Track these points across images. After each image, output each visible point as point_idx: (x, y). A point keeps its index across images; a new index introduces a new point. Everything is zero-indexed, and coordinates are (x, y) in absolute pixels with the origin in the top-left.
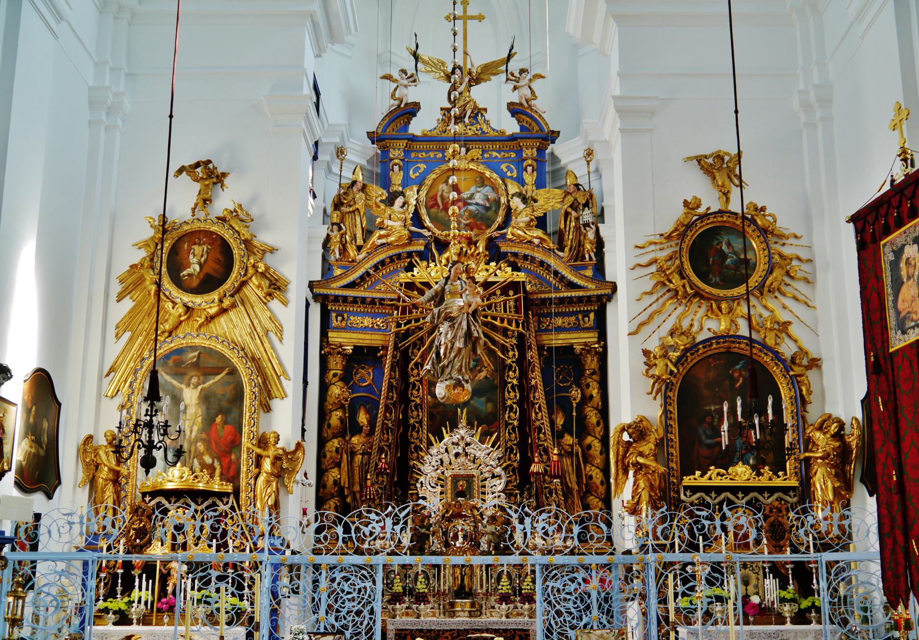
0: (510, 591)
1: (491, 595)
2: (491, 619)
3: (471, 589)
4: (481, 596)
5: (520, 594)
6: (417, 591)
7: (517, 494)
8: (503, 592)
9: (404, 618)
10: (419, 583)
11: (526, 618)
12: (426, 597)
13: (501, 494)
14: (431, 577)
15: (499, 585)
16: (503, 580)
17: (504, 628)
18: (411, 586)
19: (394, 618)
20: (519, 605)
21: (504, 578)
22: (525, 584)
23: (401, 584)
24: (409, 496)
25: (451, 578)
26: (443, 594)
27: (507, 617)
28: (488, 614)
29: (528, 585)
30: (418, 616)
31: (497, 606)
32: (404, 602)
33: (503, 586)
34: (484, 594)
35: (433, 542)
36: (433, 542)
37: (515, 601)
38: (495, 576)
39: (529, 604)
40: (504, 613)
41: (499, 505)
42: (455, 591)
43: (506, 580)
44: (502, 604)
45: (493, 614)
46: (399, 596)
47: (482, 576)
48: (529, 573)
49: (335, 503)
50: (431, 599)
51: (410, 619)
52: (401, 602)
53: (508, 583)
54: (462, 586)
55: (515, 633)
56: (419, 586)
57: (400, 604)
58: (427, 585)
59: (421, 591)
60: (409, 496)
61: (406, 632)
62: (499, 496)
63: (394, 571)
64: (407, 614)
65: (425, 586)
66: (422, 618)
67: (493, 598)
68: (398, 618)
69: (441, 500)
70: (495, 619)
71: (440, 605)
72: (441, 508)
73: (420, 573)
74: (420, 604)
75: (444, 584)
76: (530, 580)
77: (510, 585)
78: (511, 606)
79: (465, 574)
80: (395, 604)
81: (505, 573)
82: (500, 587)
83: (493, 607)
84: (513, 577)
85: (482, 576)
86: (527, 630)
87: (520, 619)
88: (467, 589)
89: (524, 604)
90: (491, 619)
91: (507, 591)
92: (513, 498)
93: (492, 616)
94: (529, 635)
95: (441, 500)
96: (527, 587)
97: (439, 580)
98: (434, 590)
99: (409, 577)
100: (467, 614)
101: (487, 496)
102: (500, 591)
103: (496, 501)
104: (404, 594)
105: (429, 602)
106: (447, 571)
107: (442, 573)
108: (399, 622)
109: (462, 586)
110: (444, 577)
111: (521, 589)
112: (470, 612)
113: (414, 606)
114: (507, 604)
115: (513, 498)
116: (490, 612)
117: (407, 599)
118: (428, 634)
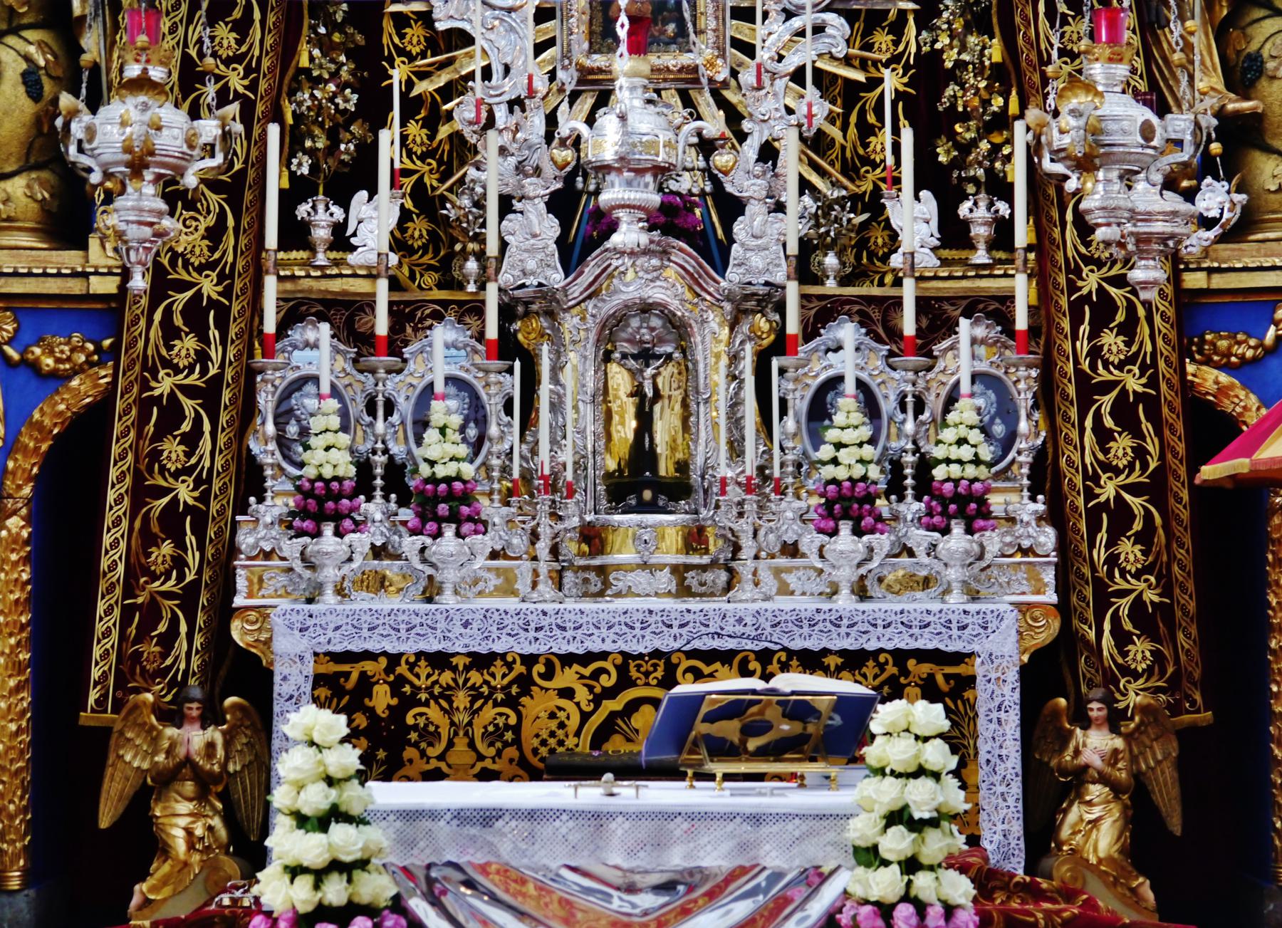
0: (874, 472)
1: (779, 490)
2: (784, 603)
3: (683, 467)
4: (734, 493)
5: (924, 485)
6: (425, 470)
7: (902, 14)
8: (841, 473)
9: (363, 602)
10: (431, 435)
11: (956, 600)
12: (467, 497)
13: (831, 17)
14: (493, 405)
15: (817, 441)
16: (839, 419)
17: (849, 644)
18: (397, 449)
19: (310, 601)
20: (919, 537)
21: (847, 408)
22: (949, 435)
23: (344, 439)
24: (388, 25)
25: (587, 411)
26: (552, 485)
27: (861, 592)
28: (766, 576)
29: (961, 442)
30: (431, 593)
31: (810, 541)
32: (358, 526)
33: (839, 446)
34: (748, 488)
35: (504, 245)
36: (504, 245)
37: (896, 517)
38: (800, 403)
39: (970, 531)
40: (846, 575)
41: (817, 72)
42: (608, 475)
43: (857, 417)
44: (834, 533)
45: (791, 579)
46: (338, 497)
47: (735, 404)
48: (965, 387)
49: (27, 58)
50: (491, 509)
51: (387, 603)
52: (344, 522)
53: (866, 432)
54: (642, 453)
55: (905, 672)
56: (434, 446)
57: (339, 533)
58: (477, 446)
59: (441, 471)
60: (388, 25)
61: (369, 666)
62: (819, 29)
63: (315, 379)
64: (380, 583)
65: (463, 450)
66: (448, 600)
67: (789, 507)
68: (330, 598)
69: (539, 49)
70: (806, 605)
71: (534, 536)
72: (541, 85)
73: (439, 387)
74: (438, 535)
75: (554, 442)
76: (973, 418)
77: (872, 441)
78: (882, 542)
79: (657, 396)
80: (317, 534)
81: (849, 386)
82: (826, 452)
83: (791, 550)
84: (888, 405)
85: (735, 404)
86: (959, 658)
87: (919, 604)
88: (665, 468)
89: (946, 531)
90: (784, 603)
91: (858, 471)
92: (883, 39)
93: (785, 590)
94: (970, 681)
95: (539, 49)
96: (955, 452)
97: (528, 421)
98: (505, 470)
99: (390, 407)
100: (665, 580)
101: (760, 29)
102: (828, 472)
103: (804, 54)
104: (364, 484)
105: (482, 526)
106: (567, 377)
107: (545, 390)
108: (334, 621)
109: (642, 453)
110: (556, 407)
111: (925, 465)
112: (679, 571)
113: (410, 545)
114: (858, 532)
115: (883, 39)
116: (777, 572)
117: (374, 509)
118: (475, 678)
